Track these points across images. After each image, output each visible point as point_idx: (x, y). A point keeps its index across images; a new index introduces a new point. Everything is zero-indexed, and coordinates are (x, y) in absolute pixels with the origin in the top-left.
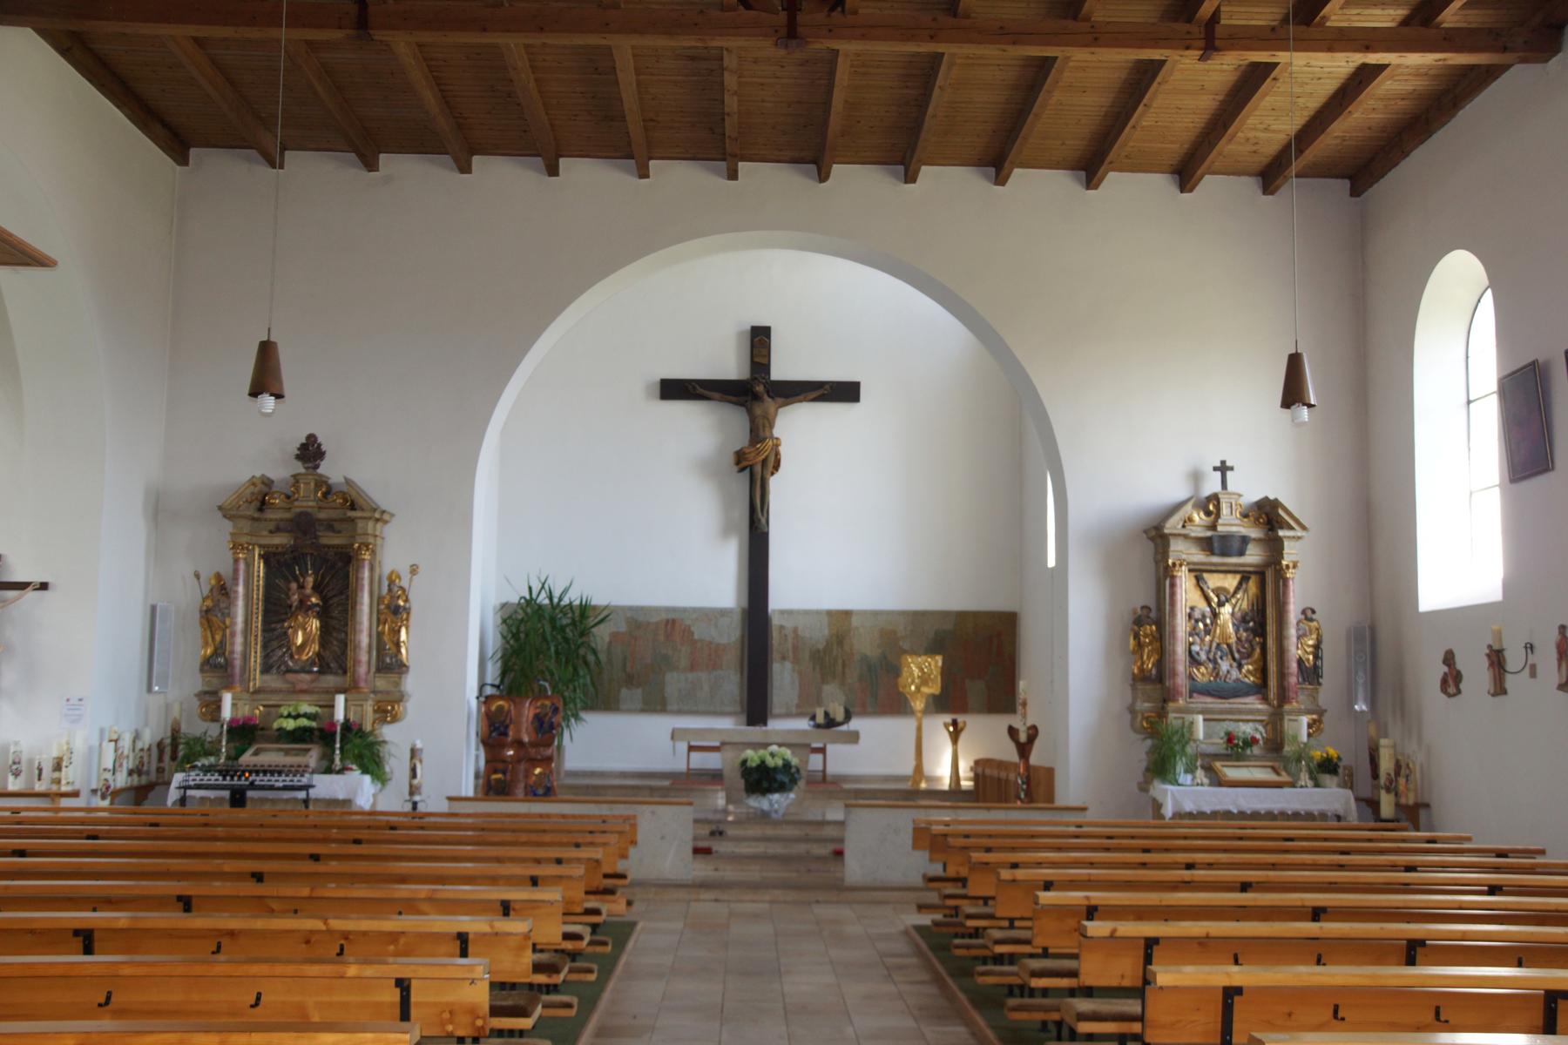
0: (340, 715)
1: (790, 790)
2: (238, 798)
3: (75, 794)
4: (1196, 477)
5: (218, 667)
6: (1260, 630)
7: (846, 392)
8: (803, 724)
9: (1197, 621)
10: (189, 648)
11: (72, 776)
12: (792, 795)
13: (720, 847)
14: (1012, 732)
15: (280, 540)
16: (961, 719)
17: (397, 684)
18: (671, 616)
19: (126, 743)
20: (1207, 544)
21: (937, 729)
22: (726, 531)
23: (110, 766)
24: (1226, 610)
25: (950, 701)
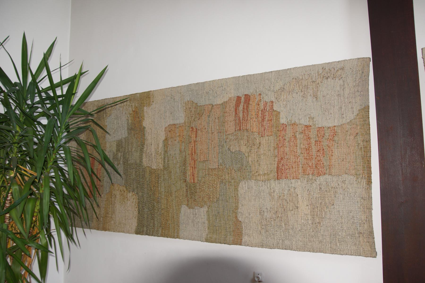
18: (241, 93)
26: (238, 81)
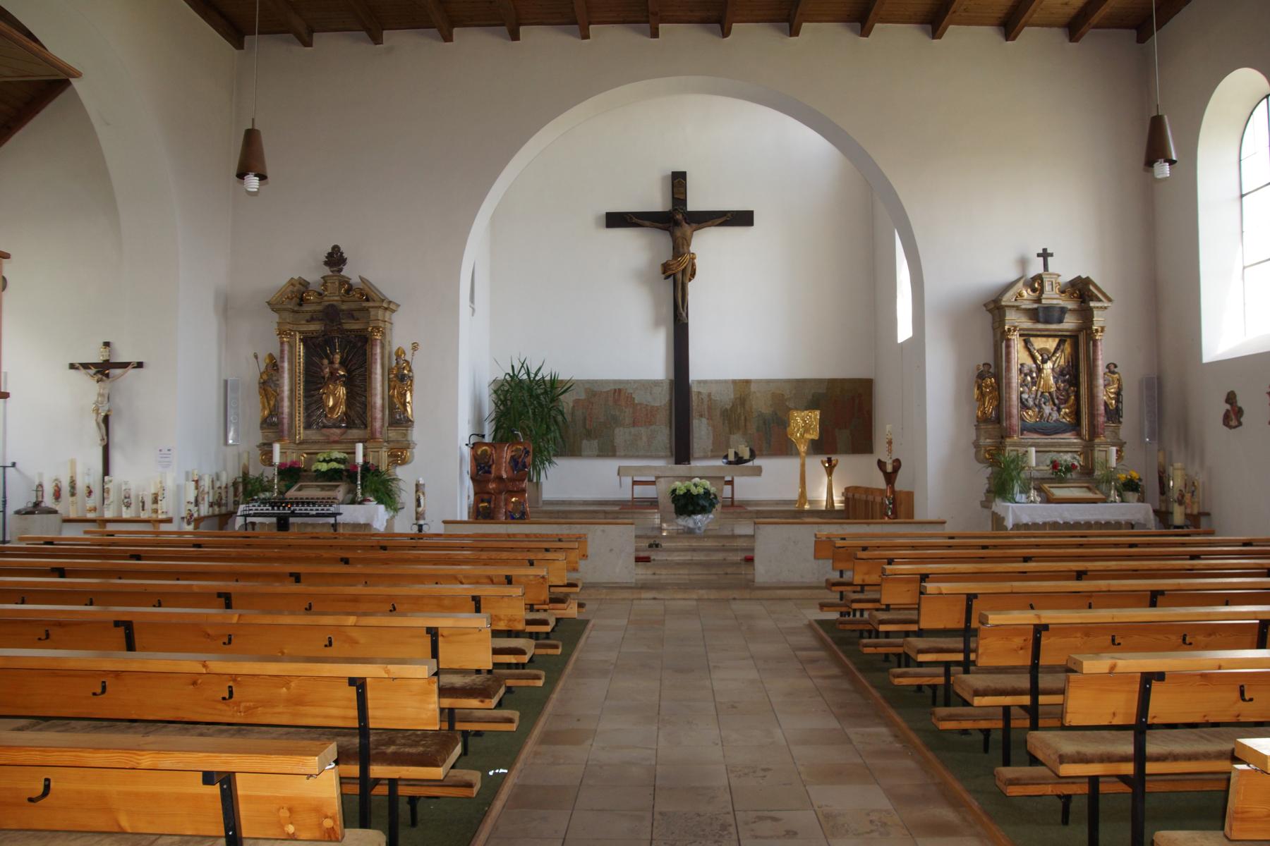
0: (360, 459)
1: (710, 512)
2: (283, 524)
3: (169, 521)
4: (1023, 263)
5: (272, 424)
6: (1074, 382)
7: (743, 219)
8: (720, 463)
9: (1026, 375)
10: (251, 409)
11: (167, 507)
12: (711, 516)
13: (656, 556)
14: (881, 465)
15: (315, 327)
16: (834, 458)
17: (405, 435)
18: (617, 387)
19: (206, 483)
20: (1034, 315)
21: (816, 464)
22: (657, 323)
23: (193, 500)
24: (1049, 365)
25: (824, 446)
26: (615, 382)
